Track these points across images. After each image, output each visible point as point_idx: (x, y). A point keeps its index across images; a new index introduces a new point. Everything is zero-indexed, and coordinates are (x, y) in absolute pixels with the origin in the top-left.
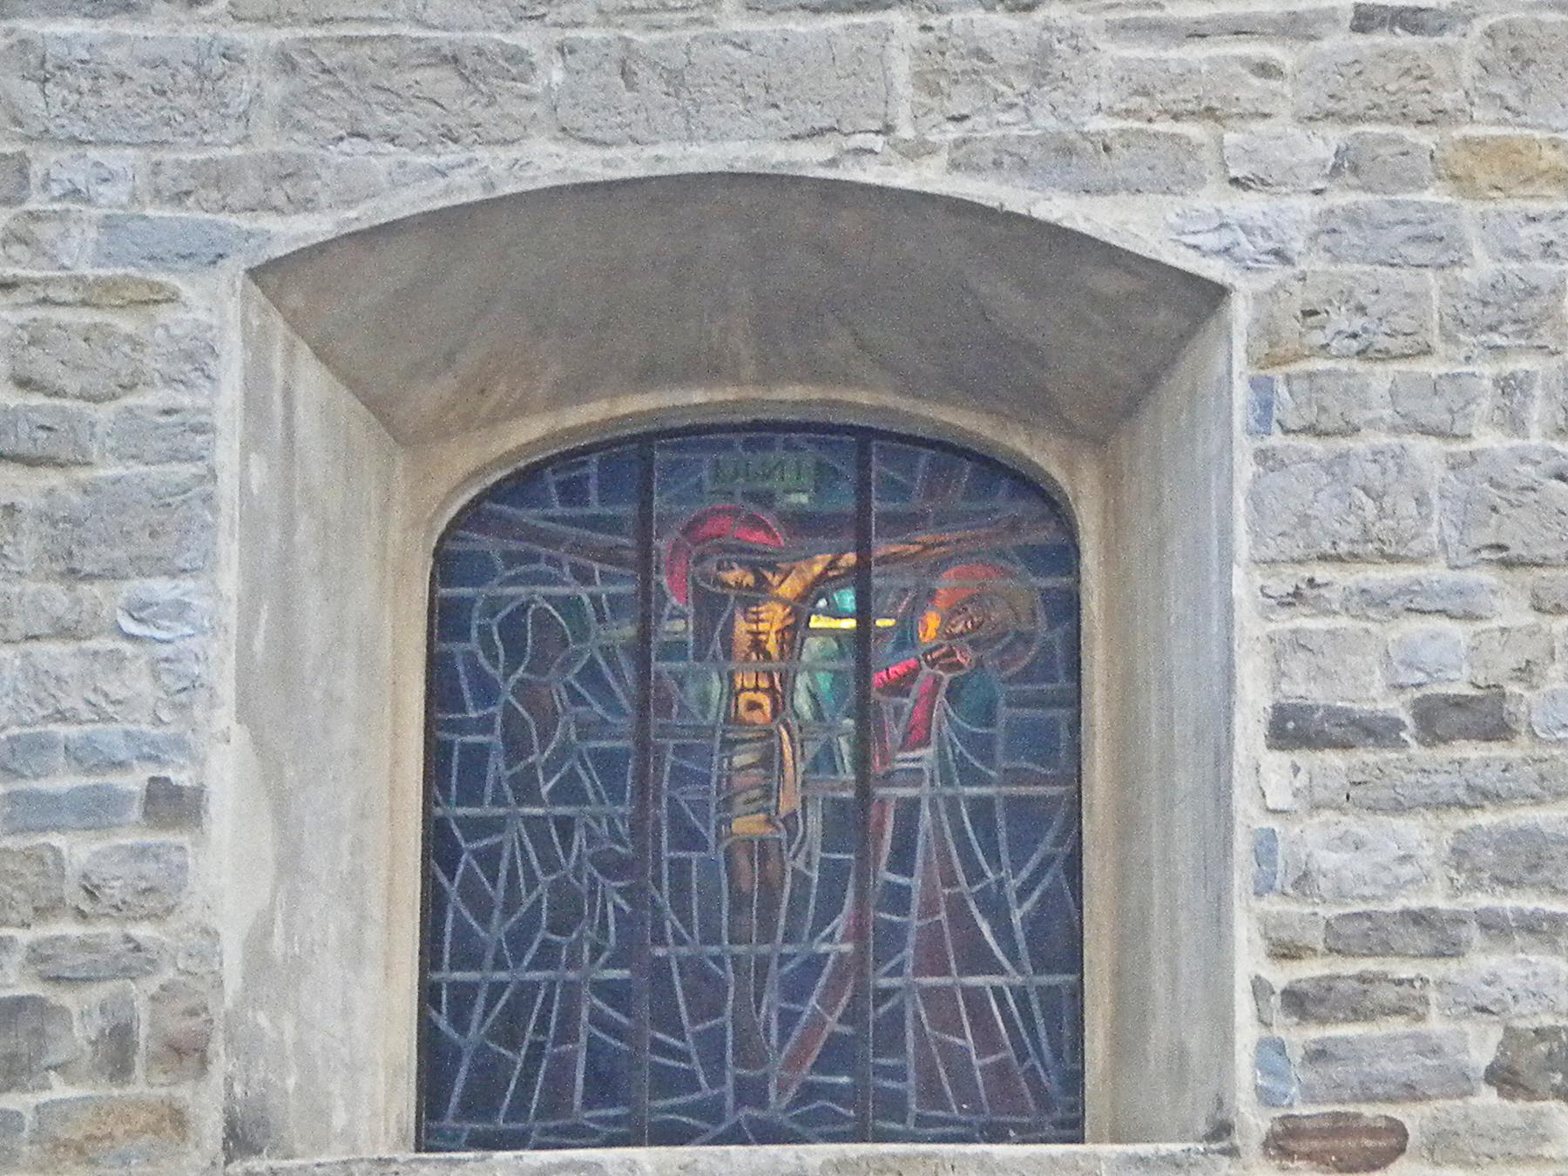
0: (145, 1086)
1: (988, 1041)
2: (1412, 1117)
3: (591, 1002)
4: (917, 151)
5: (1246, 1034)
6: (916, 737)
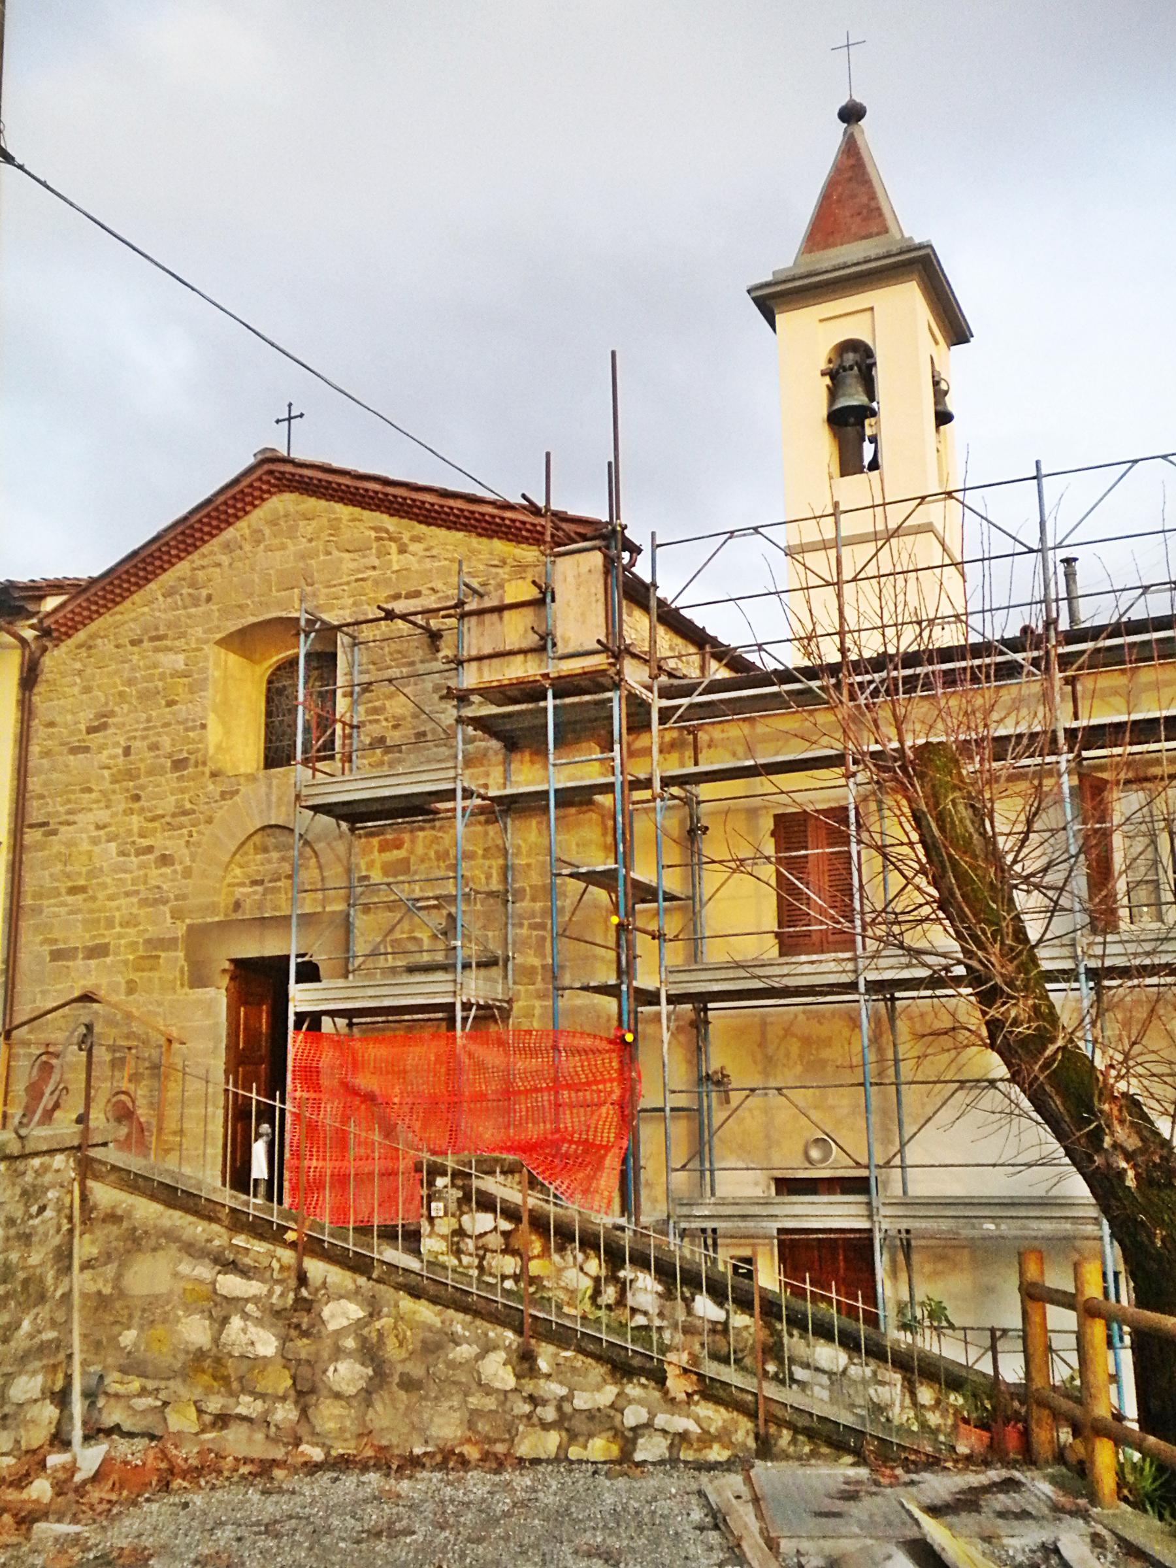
0: (200, 768)
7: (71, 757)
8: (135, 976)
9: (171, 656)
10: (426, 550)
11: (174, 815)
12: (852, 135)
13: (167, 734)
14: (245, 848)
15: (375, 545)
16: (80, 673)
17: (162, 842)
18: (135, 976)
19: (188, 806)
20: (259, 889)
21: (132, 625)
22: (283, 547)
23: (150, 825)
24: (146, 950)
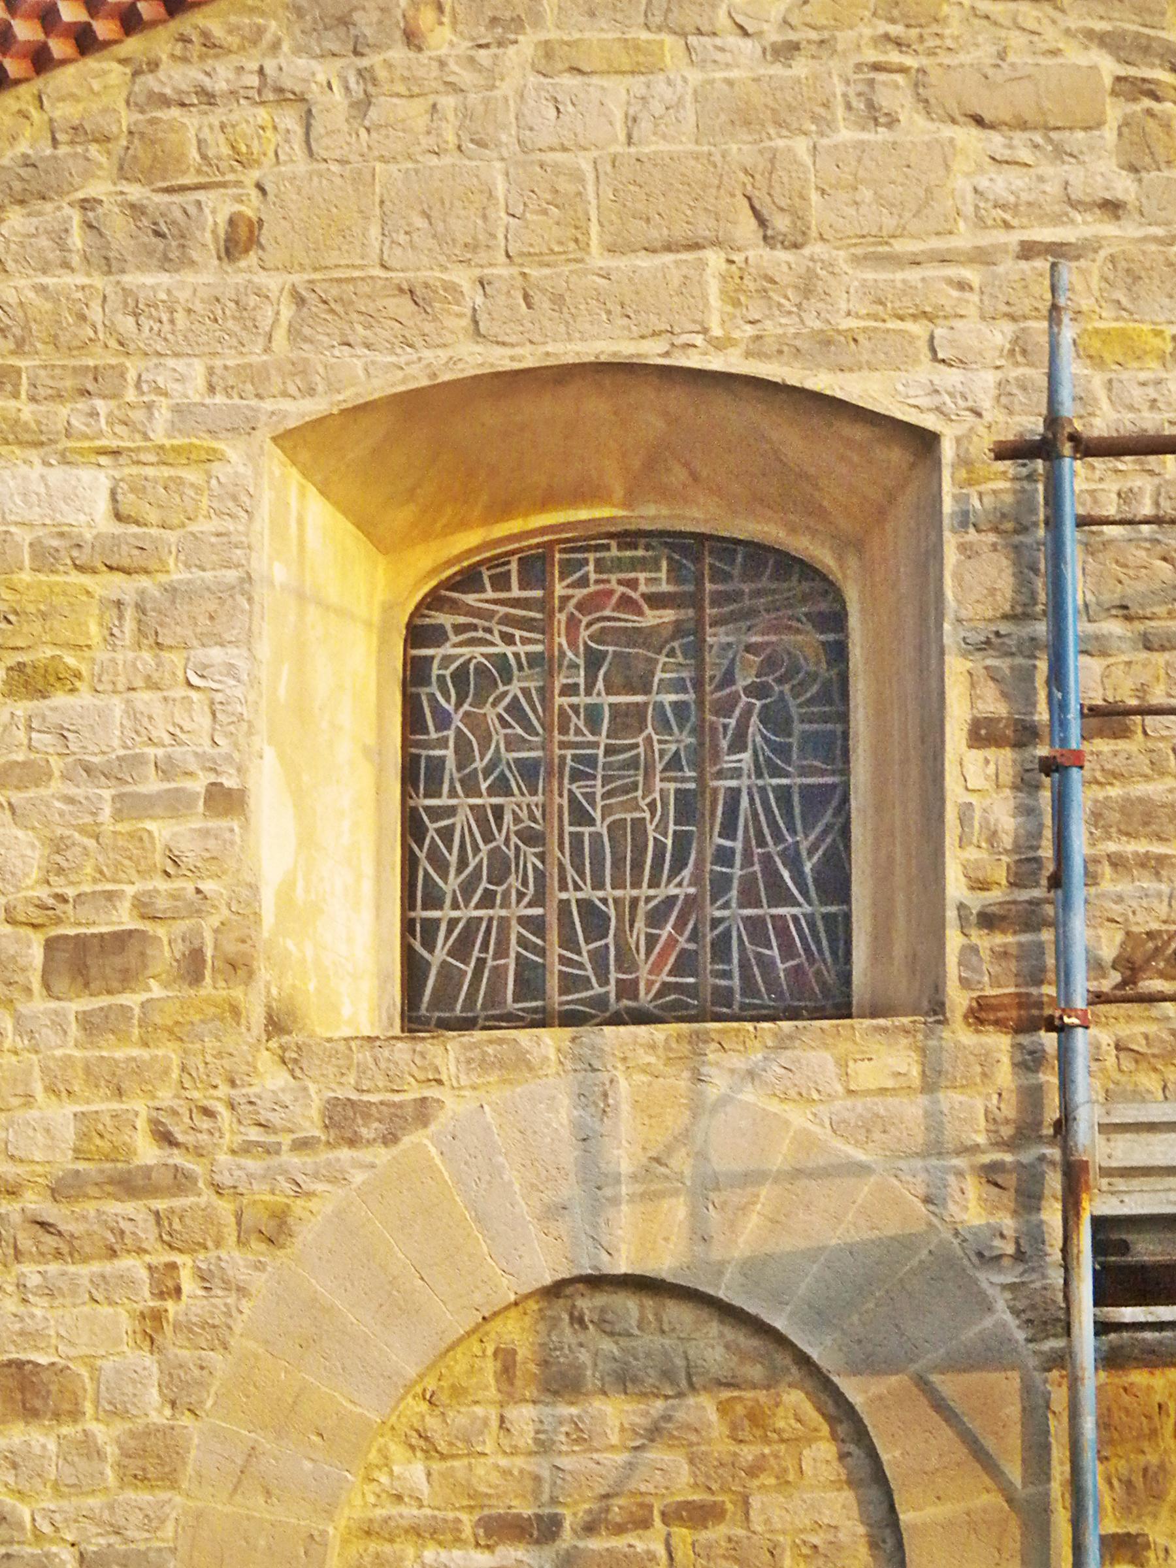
1: (788, 950)
3: (516, 929)
5: (954, 940)
6: (739, 744)
14: (459, 1363)
15: (1115, 111)
19: (148, 1152)
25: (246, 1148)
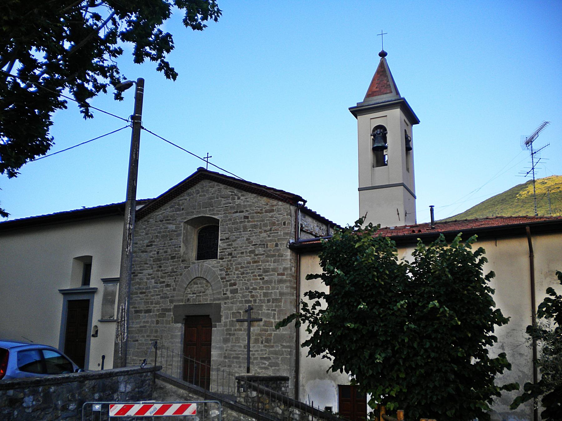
0: (179, 259)
2: (224, 257)
4: (208, 214)
7: (142, 254)
8: (159, 319)
9: (171, 226)
10: (245, 199)
11: (171, 272)
12: (383, 61)
13: (170, 248)
14: (191, 283)
16: (145, 229)
17: (167, 280)
18: (159, 319)
19: (175, 270)
20: (195, 295)
21: (160, 216)
22: (204, 195)
23: (165, 275)
24: (162, 312)
25: (180, 269)
